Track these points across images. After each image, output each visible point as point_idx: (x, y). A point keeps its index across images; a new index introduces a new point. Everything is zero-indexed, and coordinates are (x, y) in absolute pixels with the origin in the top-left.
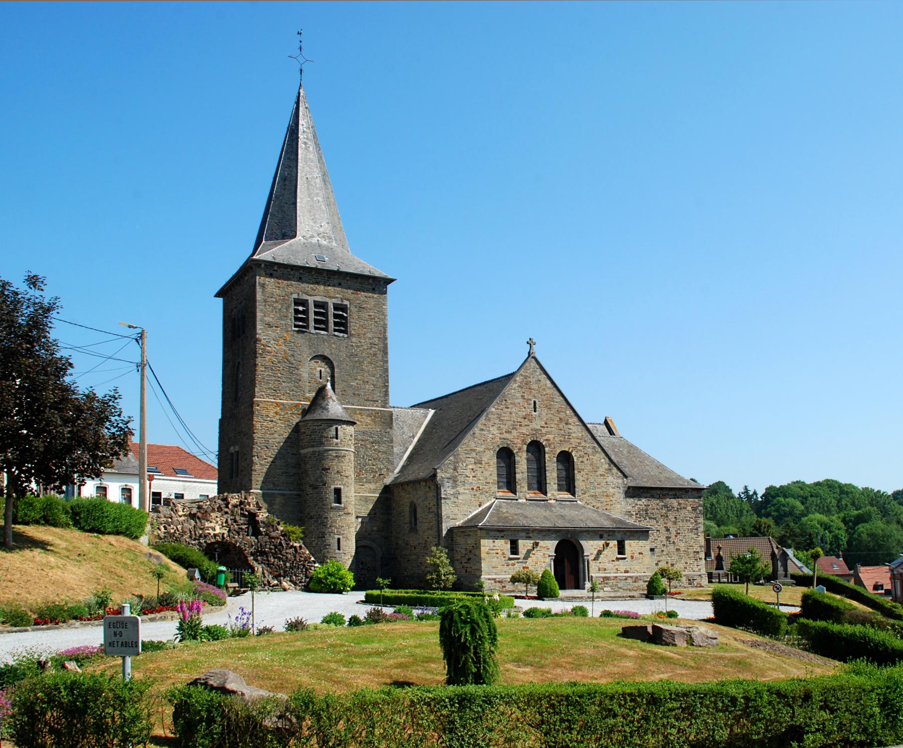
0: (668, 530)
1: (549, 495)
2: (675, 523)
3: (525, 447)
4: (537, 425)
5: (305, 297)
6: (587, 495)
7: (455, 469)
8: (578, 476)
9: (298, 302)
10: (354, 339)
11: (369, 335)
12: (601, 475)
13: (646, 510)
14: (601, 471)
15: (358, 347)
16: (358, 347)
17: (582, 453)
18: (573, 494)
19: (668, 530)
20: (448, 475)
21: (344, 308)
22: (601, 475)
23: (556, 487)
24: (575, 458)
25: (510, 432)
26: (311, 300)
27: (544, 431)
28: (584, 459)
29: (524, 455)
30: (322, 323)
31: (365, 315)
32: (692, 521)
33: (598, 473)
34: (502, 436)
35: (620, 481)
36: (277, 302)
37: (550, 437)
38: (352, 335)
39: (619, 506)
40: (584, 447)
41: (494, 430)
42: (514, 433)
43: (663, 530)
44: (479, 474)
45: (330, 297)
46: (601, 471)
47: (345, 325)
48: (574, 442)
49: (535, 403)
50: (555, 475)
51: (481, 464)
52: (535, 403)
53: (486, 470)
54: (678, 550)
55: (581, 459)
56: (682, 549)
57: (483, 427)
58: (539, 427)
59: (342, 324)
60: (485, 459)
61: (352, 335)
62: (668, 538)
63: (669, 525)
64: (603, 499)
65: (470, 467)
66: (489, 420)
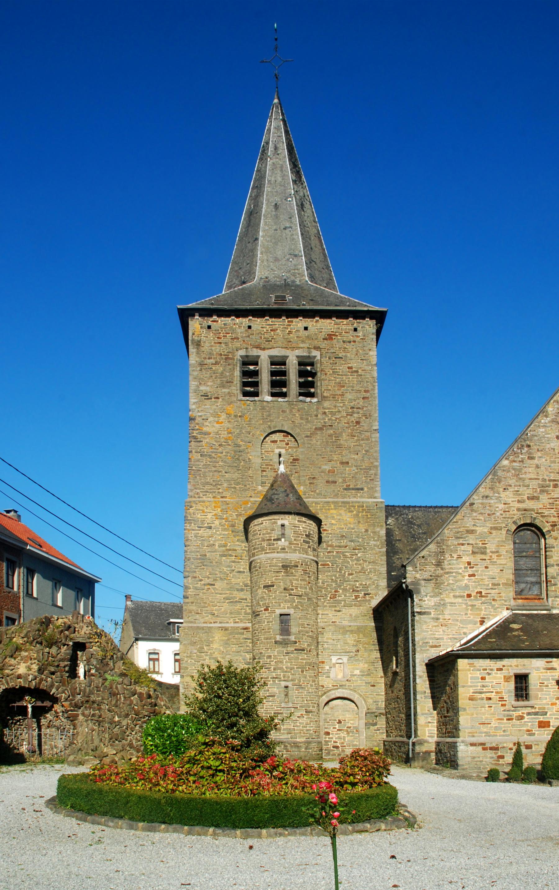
5: (255, 352)
9: (247, 362)
15: (333, 414)
16: (333, 414)
26: (264, 357)
30: (279, 385)
31: (342, 368)
36: (216, 363)
38: (324, 398)
59: (307, 387)
61: (324, 398)
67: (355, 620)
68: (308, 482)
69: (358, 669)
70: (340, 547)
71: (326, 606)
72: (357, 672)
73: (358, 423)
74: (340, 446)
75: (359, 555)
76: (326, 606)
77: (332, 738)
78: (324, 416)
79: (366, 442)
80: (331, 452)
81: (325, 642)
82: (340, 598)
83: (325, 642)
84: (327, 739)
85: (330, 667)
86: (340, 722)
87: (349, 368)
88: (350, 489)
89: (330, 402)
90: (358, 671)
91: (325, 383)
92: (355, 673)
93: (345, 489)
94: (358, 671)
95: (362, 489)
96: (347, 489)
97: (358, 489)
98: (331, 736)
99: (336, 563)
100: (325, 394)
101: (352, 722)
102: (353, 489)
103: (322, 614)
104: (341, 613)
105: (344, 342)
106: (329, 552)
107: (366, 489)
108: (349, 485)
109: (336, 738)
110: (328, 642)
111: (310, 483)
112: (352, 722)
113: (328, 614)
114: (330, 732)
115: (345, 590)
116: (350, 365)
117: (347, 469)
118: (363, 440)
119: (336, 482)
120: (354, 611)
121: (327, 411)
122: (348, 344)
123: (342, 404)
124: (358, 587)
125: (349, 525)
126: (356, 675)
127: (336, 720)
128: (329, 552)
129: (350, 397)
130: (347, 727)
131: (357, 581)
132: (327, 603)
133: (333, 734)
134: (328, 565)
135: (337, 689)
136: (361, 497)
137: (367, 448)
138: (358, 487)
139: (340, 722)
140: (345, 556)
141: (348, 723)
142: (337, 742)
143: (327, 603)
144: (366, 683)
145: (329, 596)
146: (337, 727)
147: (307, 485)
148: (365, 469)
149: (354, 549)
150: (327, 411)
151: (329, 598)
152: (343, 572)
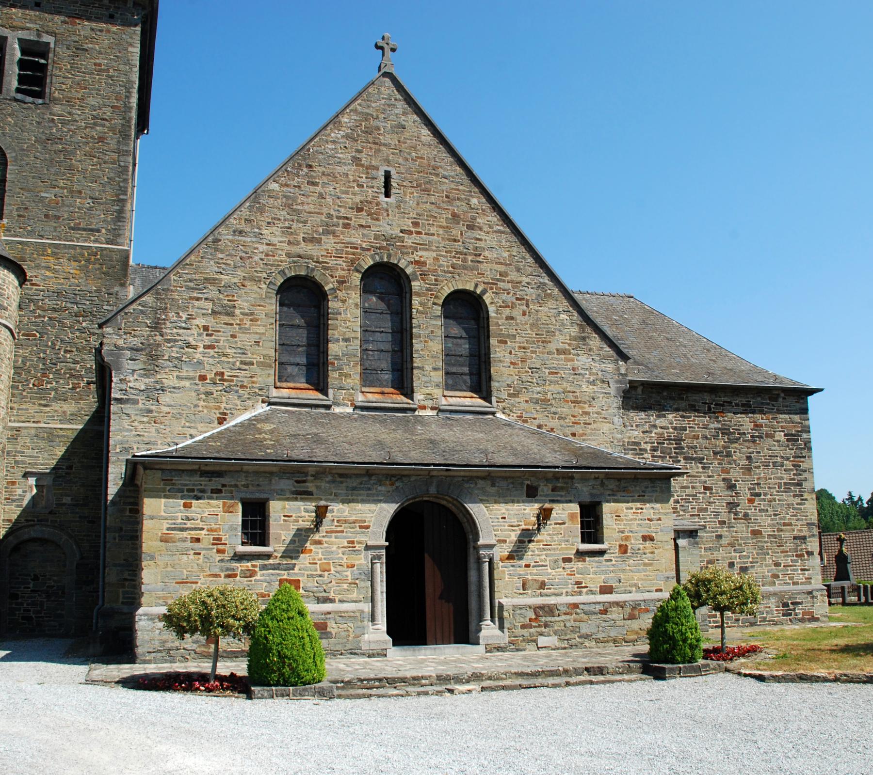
0: (731, 487)
1: (418, 396)
2: (748, 470)
3: (356, 278)
4: (390, 225)
6: (522, 399)
7: (156, 326)
8: (499, 352)
10: (57, 109)
11: (92, 101)
12: (559, 352)
13: (679, 440)
14: (559, 341)
15: (64, 123)
16: (64, 123)
17: (510, 298)
18: (487, 398)
19: (731, 487)
20: (136, 342)
21: (42, 50)
22: (559, 352)
23: (438, 377)
24: (491, 309)
25: (319, 241)
27: (409, 241)
28: (517, 313)
29: (355, 297)
31: (86, 63)
32: (788, 465)
33: (552, 347)
34: (295, 249)
35: (610, 367)
37: (427, 256)
38: (55, 101)
39: (606, 427)
40: (516, 284)
41: (274, 235)
42: (329, 243)
43: (719, 486)
44: (223, 340)
45: (14, 28)
46: (559, 341)
47: (41, 81)
48: (489, 270)
49: (388, 176)
50: (436, 346)
51: (231, 314)
52: (388, 176)
53: (244, 330)
54: (756, 533)
55: (507, 312)
56: (767, 531)
57: (243, 226)
58: (396, 232)
60: (243, 304)
61: (55, 101)
62: (732, 506)
63: (735, 474)
64: (565, 410)
65: (200, 321)
66: (262, 211)
67: (70, 421)
68: (15, 213)
69: (68, 496)
70: (54, 310)
71: (26, 397)
72: (67, 500)
73: (101, 139)
74: (70, 168)
75: (84, 324)
76: (26, 397)
77: (22, 604)
78: (51, 125)
79: (111, 166)
80: (56, 174)
81: (19, 452)
82: (49, 386)
83: (19, 452)
84: (14, 606)
85: (25, 492)
86: (36, 578)
87: (95, 64)
88: (79, 229)
89: (64, 107)
90: (69, 498)
91: (59, 81)
92: (64, 501)
93: (73, 229)
94: (69, 498)
95: (98, 231)
96: (76, 228)
97: (92, 230)
98: (20, 600)
99: (47, 334)
100: (56, 95)
101: (55, 578)
102: (84, 230)
103: (19, 409)
104: (48, 409)
105: (92, 29)
106: (40, 316)
107: (104, 231)
108: (80, 224)
109: (28, 604)
110: (23, 452)
111: (19, 216)
112: (55, 578)
113: (27, 409)
114: (19, 593)
115: (57, 373)
116: (98, 61)
117: (78, 200)
118: (105, 163)
119: (59, 218)
120: (69, 407)
121: (55, 118)
122: (98, 33)
123: (79, 112)
124: (78, 371)
125: (72, 280)
126: (65, 504)
127: (30, 575)
128: (40, 316)
129: (93, 103)
130: (48, 587)
131: (78, 362)
132: (28, 393)
133: (24, 597)
134: (35, 335)
135: (33, 526)
136: (96, 241)
137: (112, 175)
138: (93, 227)
139: (36, 578)
140: (63, 325)
141: (50, 579)
142: (29, 611)
143: (28, 393)
144: (80, 517)
145: (32, 381)
146: (31, 585)
147: (14, 218)
148: (106, 203)
149: (76, 316)
150: (55, 118)
151: (31, 386)
152: (57, 347)
